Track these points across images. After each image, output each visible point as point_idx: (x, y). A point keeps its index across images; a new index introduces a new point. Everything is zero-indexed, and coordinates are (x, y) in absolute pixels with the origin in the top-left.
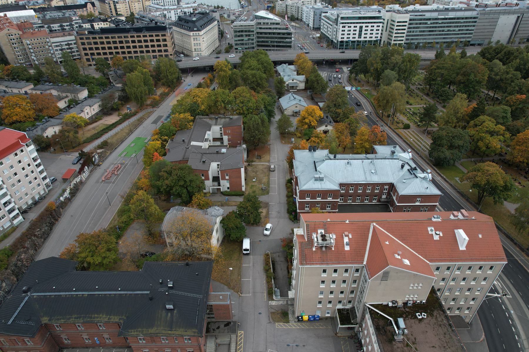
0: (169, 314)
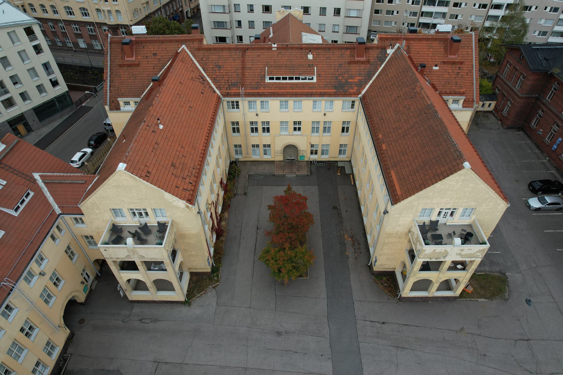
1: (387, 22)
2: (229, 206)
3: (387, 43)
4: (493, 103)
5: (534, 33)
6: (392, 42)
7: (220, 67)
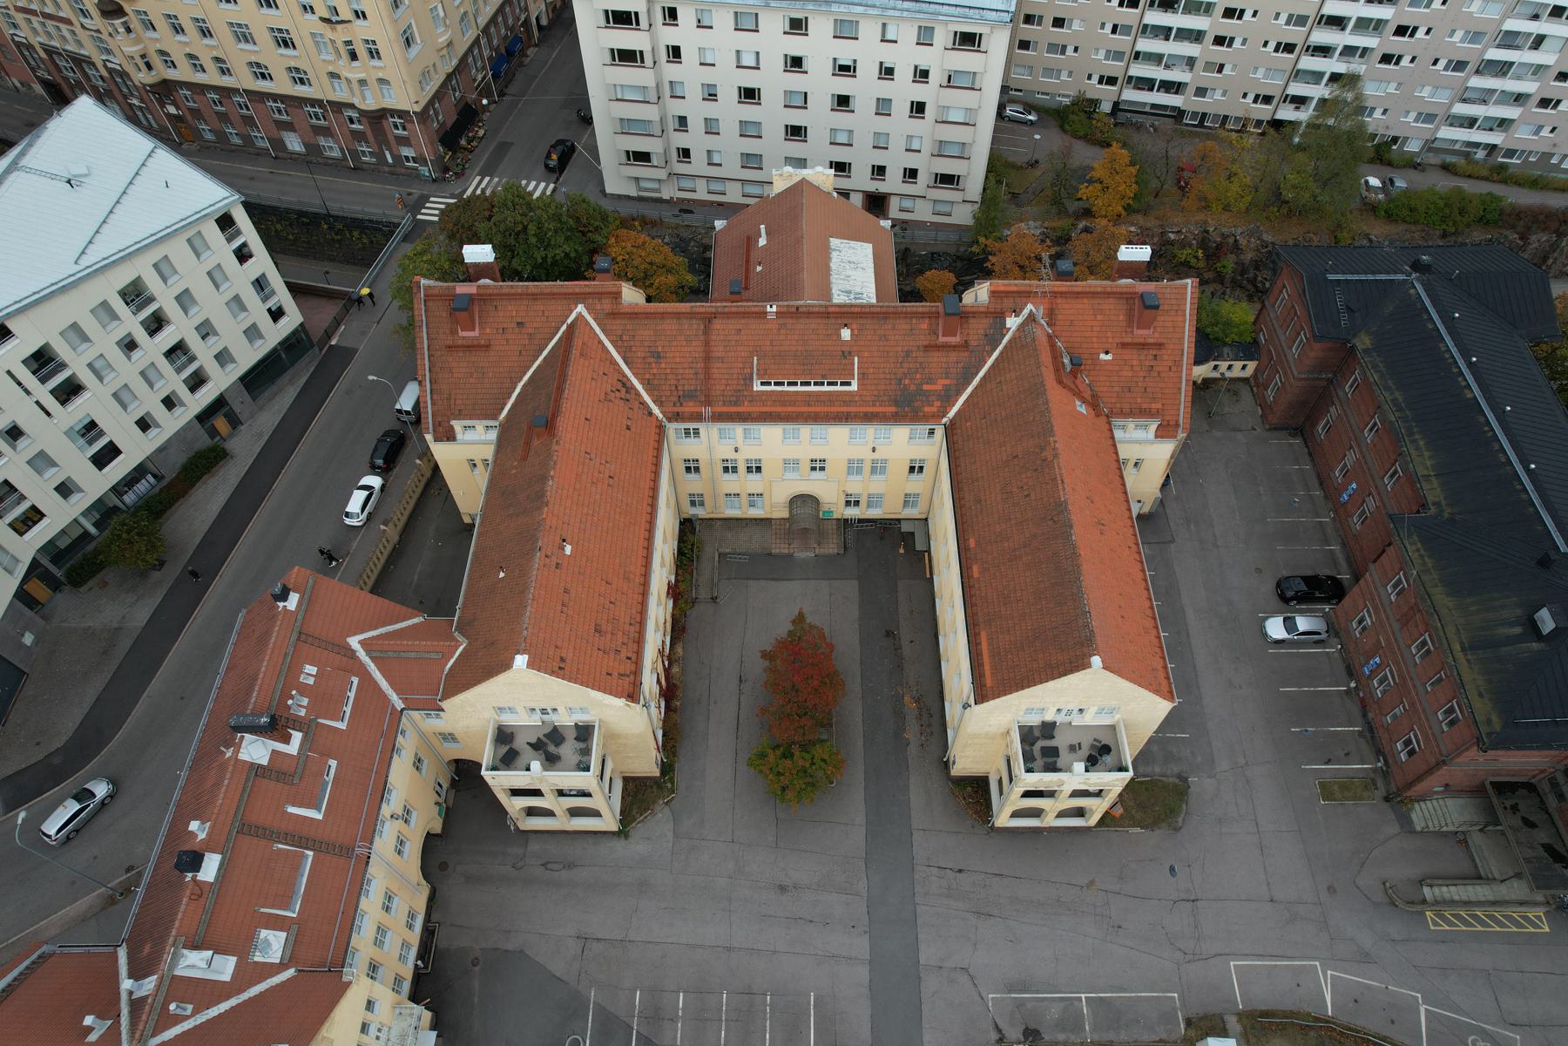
0: (1517, 630)
1: (1048, 72)
2: (684, 629)
3: (1008, 303)
4: (1252, 365)
5: (1451, 36)
6: (1018, 300)
7: (658, 356)
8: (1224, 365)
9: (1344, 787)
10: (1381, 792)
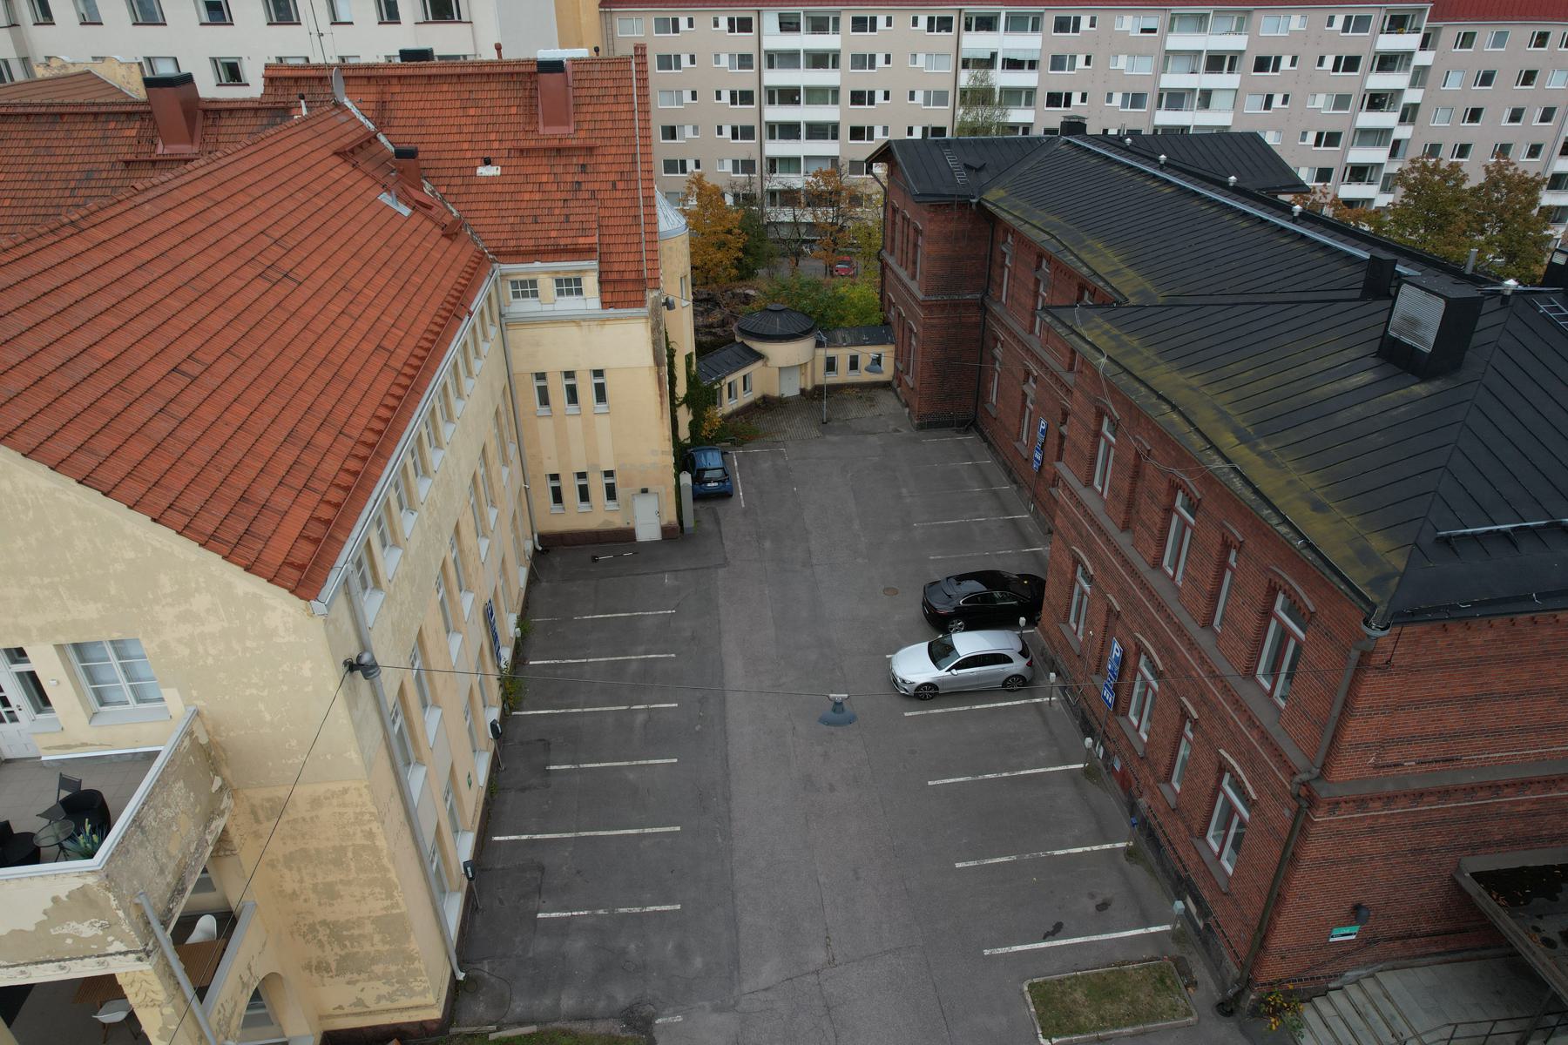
4: (887, 352)
8: (843, 355)
9: (1104, 989)
10: (1207, 989)
